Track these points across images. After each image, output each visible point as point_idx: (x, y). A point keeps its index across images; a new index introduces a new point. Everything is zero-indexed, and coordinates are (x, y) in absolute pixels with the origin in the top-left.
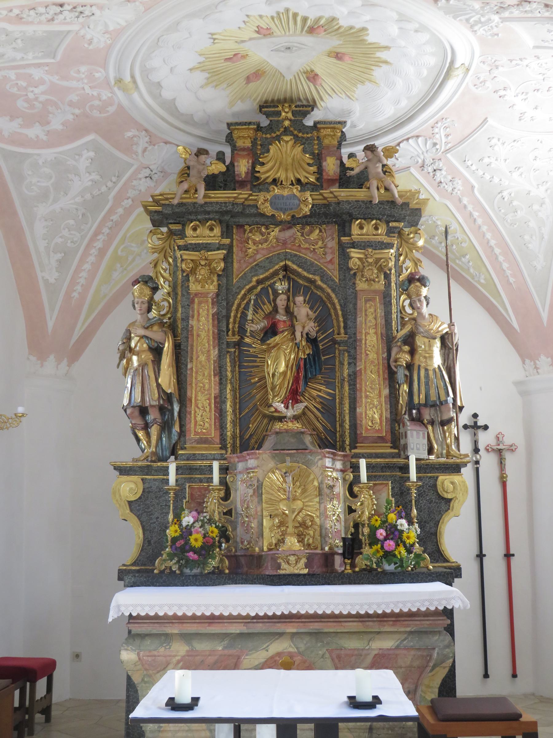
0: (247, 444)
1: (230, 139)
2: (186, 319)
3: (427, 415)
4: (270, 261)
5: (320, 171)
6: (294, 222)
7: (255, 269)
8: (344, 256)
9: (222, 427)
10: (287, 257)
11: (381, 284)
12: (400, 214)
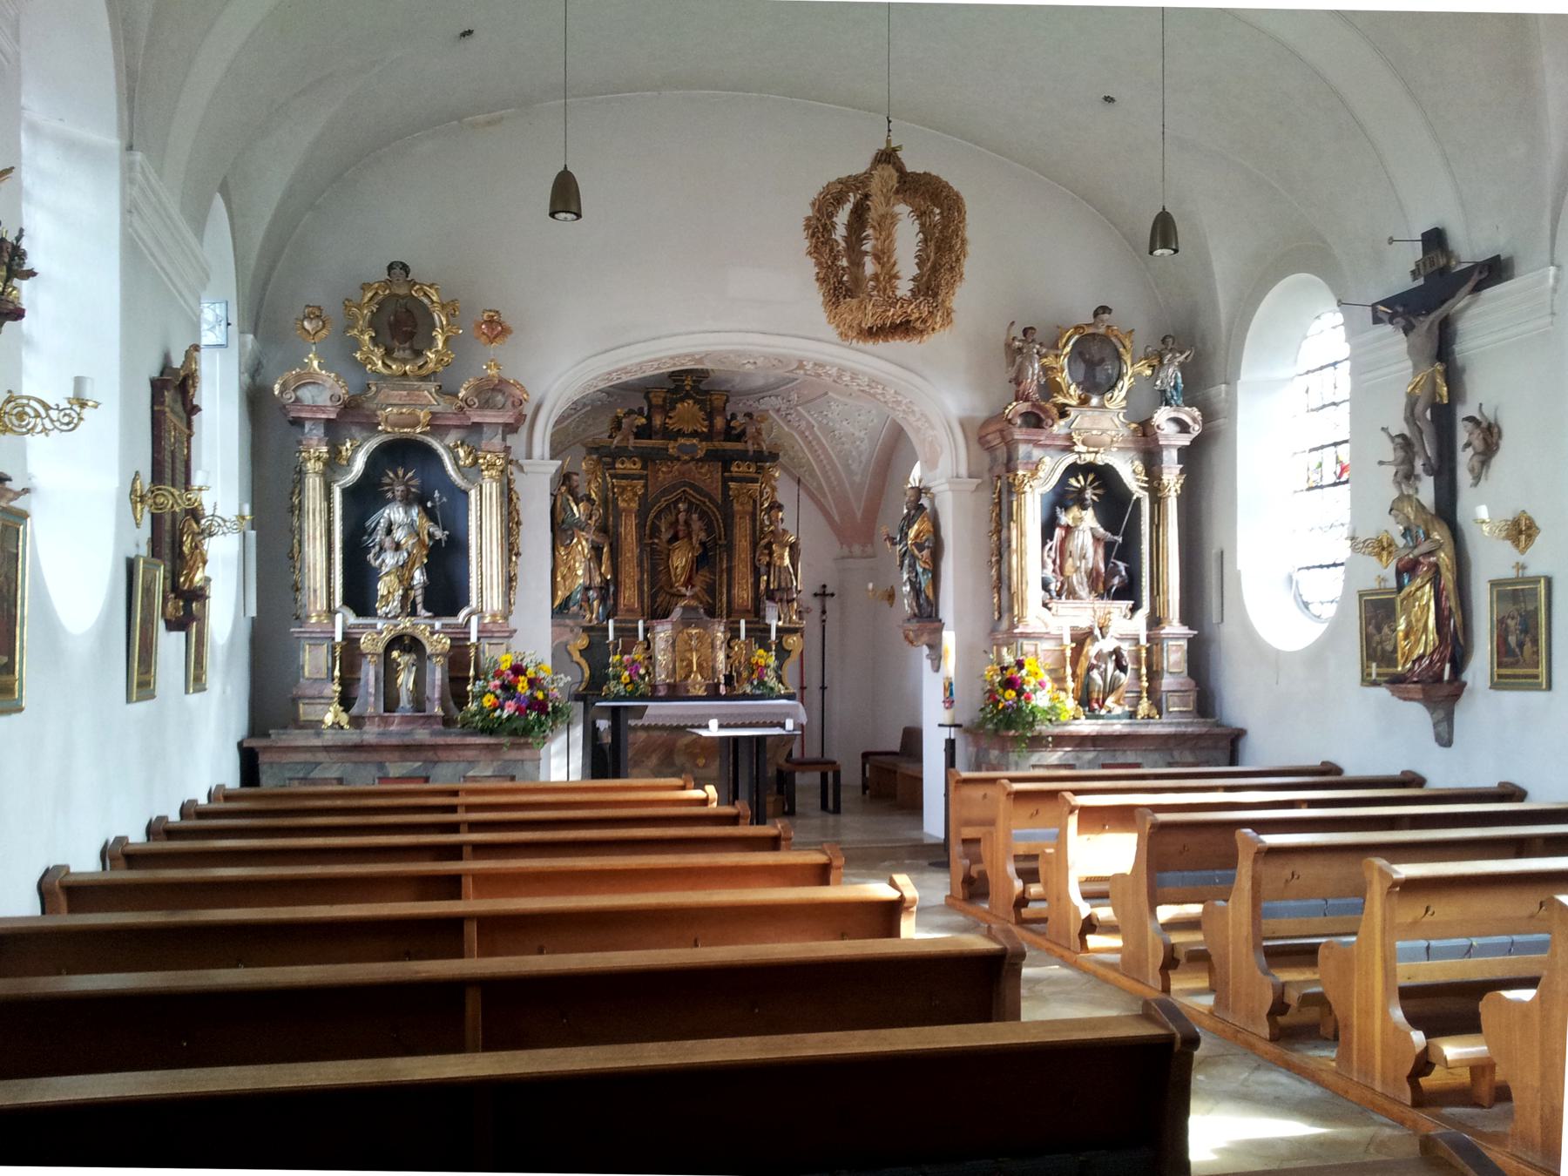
0: (657, 613)
1: (647, 397)
2: (616, 526)
3: (778, 595)
4: (674, 487)
5: (711, 426)
6: (693, 459)
7: (665, 492)
8: (726, 488)
9: (641, 601)
10: (685, 484)
11: (749, 508)
12: (765, 458)
